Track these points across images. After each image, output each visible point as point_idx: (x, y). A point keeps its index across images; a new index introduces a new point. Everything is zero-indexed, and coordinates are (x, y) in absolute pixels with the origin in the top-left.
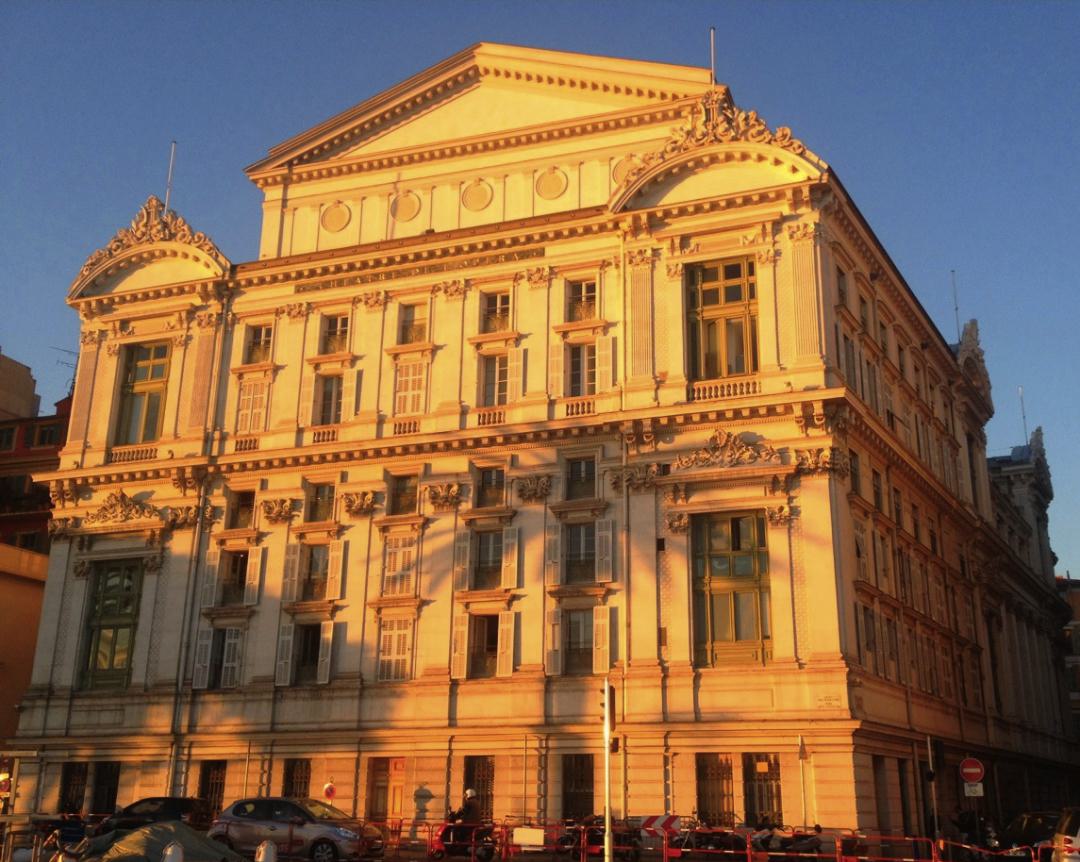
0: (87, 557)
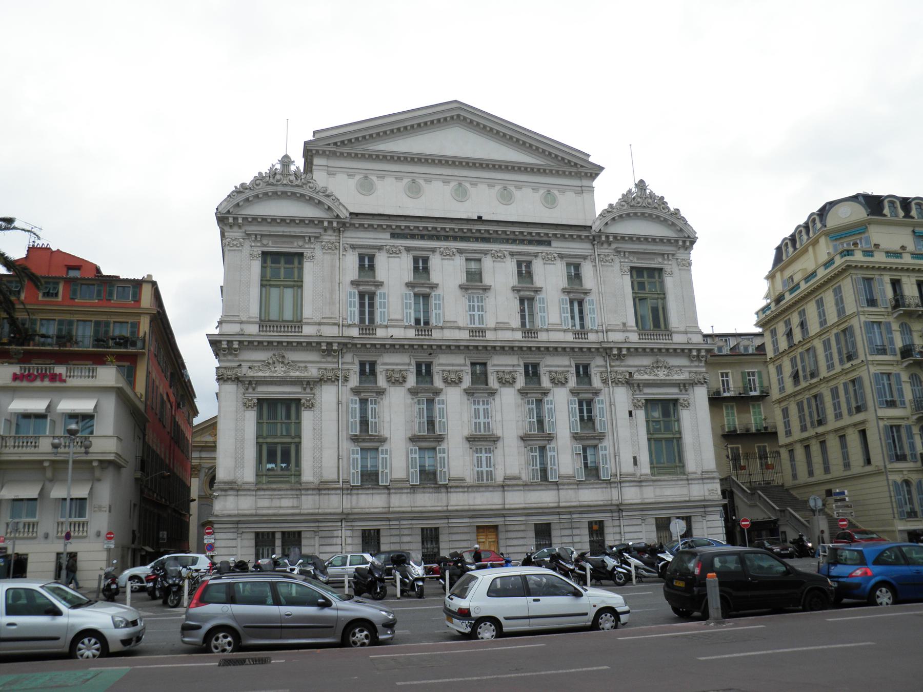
0: (254, 396)
